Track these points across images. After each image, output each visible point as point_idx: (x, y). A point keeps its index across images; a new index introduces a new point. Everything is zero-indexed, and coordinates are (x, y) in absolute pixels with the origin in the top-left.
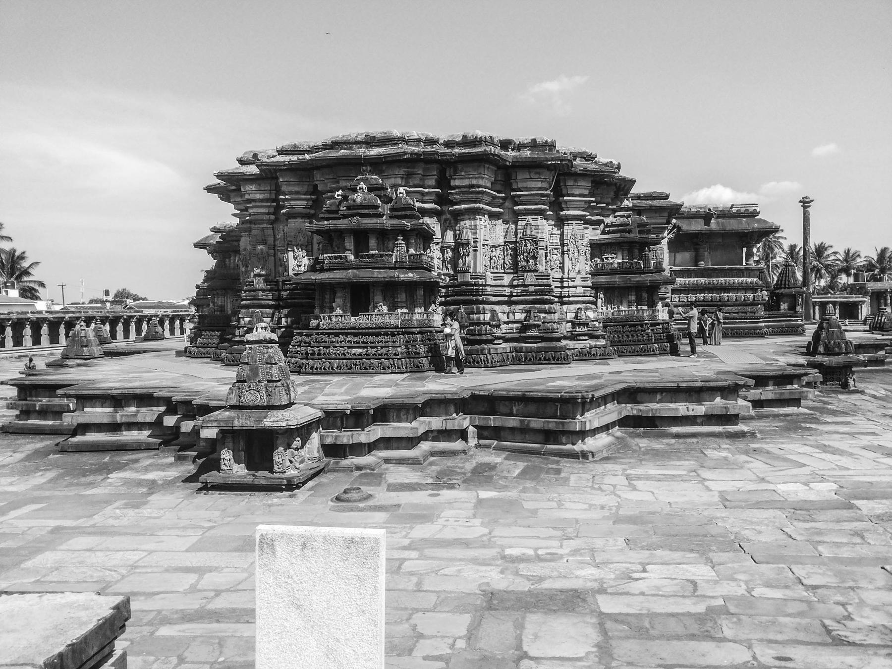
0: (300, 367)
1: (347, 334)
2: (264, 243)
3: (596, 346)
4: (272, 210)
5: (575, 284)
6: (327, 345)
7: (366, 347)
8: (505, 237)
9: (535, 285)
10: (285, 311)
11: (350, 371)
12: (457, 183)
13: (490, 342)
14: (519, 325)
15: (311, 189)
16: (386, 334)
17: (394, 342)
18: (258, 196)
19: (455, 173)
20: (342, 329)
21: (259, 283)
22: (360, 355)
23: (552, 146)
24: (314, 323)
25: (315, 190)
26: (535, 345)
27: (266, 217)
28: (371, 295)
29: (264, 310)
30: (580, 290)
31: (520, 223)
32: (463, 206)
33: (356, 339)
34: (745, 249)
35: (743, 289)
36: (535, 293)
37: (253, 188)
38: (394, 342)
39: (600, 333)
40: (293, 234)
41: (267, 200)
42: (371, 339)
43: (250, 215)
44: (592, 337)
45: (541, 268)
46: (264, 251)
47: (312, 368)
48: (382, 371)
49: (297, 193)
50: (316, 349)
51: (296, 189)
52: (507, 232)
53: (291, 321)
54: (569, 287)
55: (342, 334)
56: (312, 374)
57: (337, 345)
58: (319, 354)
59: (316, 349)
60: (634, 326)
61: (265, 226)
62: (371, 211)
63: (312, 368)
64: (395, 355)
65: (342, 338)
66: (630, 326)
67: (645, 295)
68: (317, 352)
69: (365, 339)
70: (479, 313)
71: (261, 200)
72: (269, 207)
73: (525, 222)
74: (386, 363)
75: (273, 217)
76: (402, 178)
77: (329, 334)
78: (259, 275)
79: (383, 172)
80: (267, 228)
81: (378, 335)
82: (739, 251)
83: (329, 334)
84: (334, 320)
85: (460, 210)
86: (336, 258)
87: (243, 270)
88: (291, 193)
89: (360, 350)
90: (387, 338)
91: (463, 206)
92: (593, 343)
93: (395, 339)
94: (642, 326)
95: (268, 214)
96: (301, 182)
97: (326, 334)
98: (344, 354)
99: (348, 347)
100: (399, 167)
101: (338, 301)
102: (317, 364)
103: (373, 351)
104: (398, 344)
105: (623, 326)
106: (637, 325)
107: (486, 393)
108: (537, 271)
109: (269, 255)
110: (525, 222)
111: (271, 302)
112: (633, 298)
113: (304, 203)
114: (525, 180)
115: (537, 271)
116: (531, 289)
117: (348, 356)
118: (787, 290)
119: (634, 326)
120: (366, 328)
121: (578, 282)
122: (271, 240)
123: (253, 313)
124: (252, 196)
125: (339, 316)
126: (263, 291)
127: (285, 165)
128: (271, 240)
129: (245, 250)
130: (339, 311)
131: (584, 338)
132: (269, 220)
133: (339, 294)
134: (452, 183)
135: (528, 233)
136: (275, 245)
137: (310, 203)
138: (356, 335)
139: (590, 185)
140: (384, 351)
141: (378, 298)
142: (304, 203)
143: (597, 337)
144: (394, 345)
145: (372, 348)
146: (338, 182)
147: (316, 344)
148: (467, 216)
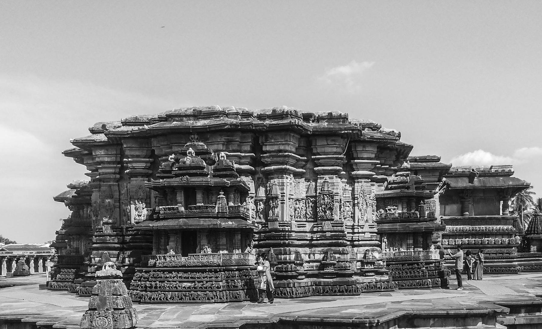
0: (140, 298)
1: (178, 271)
2: (111, 197)
3: (380, 281)
4: (117, 170)
5: (364, 230)
6: (162, 280)
7: (194, 282)
8: (307, 192)
9: (331, 232)
10: (128, 253)
11: (181, 301)
12: (268, 148)
13: (295, 277)
14: (318, 264)
15: (149, 153)
16: (210, 271)
17: (217, 277)
18: (106, 159)
19: (266, 140)
20: (174, 267)
21: (107, 230)
22: (189, 288)
23: (345, 118)
24: (151, 262)
25: (152, 154)
26: (331, 280)
27: (112, 176)
28: (198, 239)
29: (111, 252)
30: (368, 235)
31: (319, 181)
32: (273, 167)
33: (185, 275)
34: (502, 202)
35: (500, 234)
36: (331, 238)
37: (102, 152)
38: (217, 277)
39: (384, 270)
40: (134, 190)
41: (113, 163)
42: (198, 275)
43: (100, 174)
44: (378, 273)
45: (336, 217)
46: (111, 203)
47: (150, 299)
48: (207, 301)
49: (138, 156)
50: (153, 283)
52: (308, 188)
53: (133, 261)
54: (359, 233)
55: (175, 271)
56: (150, 303)
57: (170, 280)
58: (156, 287)
59: (153, 283)
60: (412, 264)
61: (112, 183)
62: (198, 171)
63: (150, 299)
64: (218, 288)
65: (174, 274)
66: (409, 264)
67: (421, 239)
68: (154, 286)
69: (193, 275)
70: (285, 254)
71: (109, 163)
72: (115, 168)
73: (323, 180)
74: (210, 294)
75: (118, 176)
76: (223, 144)
77: (164, 271)
78: (107, 223)
79: (208, 139)
80: (114, 185)
81: (203, 271)
82: (497, 203)
83: (164, 271)
84: (168, 259)
85: (271, 170)
86: (169, 209)
87: (94, 219)
88: (133, 156)
89: (189, 284)
90: (211, 274)
91: (273, 167)
92: (378, 278)
93: (217, 275)
94: (418, 265)
95: (115, 173)
96: (141, 148)
97: (162, 271)
98: (176, 287)
99: (180, 282)
100: (221, 135)
101: (171, 244)
102: (154, 295)
103: (200, 285)
104: (220, 279)
105: (403, 265)
106: (414, 264)
107: (292, 319)
108: (333, 220)
109: (115, 207)
110: (323, 180)
111: (116, 245)
112: (411, 242)
113: (144, 165)
114: (323, 146)
115: (333, 220)
116: (328, 234)
117: (179, 289)
118: (536, 236)
119: (412, 264)
120: (194, 266)
121: (366, 229)
122: (116, 195)
123: (102, 254)
124: (101, 159)
125: (172, 257)
126: (110, 236)
127: (128, 134)
128: (116, 195)
129: (95, 202)
130: (172, 252)
131: (371, 274)
132: (115, 179)
133: (172, 239)
134: (264, 149)
135: (326, 189)
136: (120, 199)
137: (149, 165)
138: (185, 272)
139: (376, 150)
140: (209, 284)
141: (204, 241)
142: (144, 165)
143: (382, 274)
144: (217, 280)
145: (199, 282)
146: (171, 148)
147: (153, 279)
148: (276, 176)
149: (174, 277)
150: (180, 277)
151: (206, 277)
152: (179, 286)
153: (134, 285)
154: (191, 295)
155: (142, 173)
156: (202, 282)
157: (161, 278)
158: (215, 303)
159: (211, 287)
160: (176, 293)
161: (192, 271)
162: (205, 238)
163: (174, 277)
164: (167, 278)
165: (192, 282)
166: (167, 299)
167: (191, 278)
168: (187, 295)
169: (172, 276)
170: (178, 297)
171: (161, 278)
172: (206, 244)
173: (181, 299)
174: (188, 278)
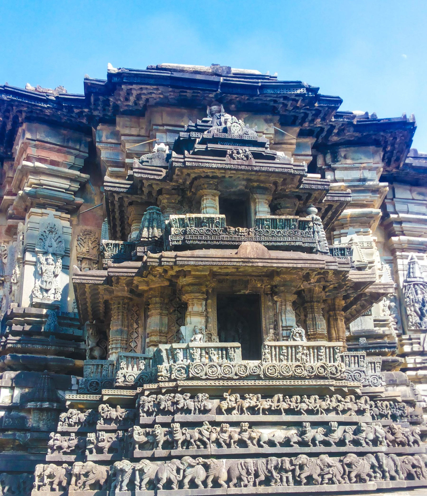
1: (243, 392)
6: (190, 418)
20: (222, 379)
40: (36, 233)
50: (160, 431)
51: (54, 157)
58: (170, 444)
69: (293, 402)
74: (363, 465)
81: (323, 393)
99: (252, 424)
127: (47, 101)
138: (267, 393)
141: (289, 318)
145: (314, 424)
147: (160, 418)
149: (229, 411)
150: (253, 410)
151: (335, 409)
152: (251, 439)
153: (60, 448)
154: (301, 467)
155: (59, 199)
156: (325, 424)
157: (188, 411)
158: (379, 491)
159: (356, 443)
160: (250, 461)
161: (289, 392)
162: (289, 308)
163: (229, 411)
164: (205, 411)
165: (288, 425)
166: (216, 484)
167: (289, 411)
168: (287, 465)
169: (225, 405)
170: (257, 475)
171: (188, 411)
172: (294, 324)
173: (267, 482)
174: (278, 412)
